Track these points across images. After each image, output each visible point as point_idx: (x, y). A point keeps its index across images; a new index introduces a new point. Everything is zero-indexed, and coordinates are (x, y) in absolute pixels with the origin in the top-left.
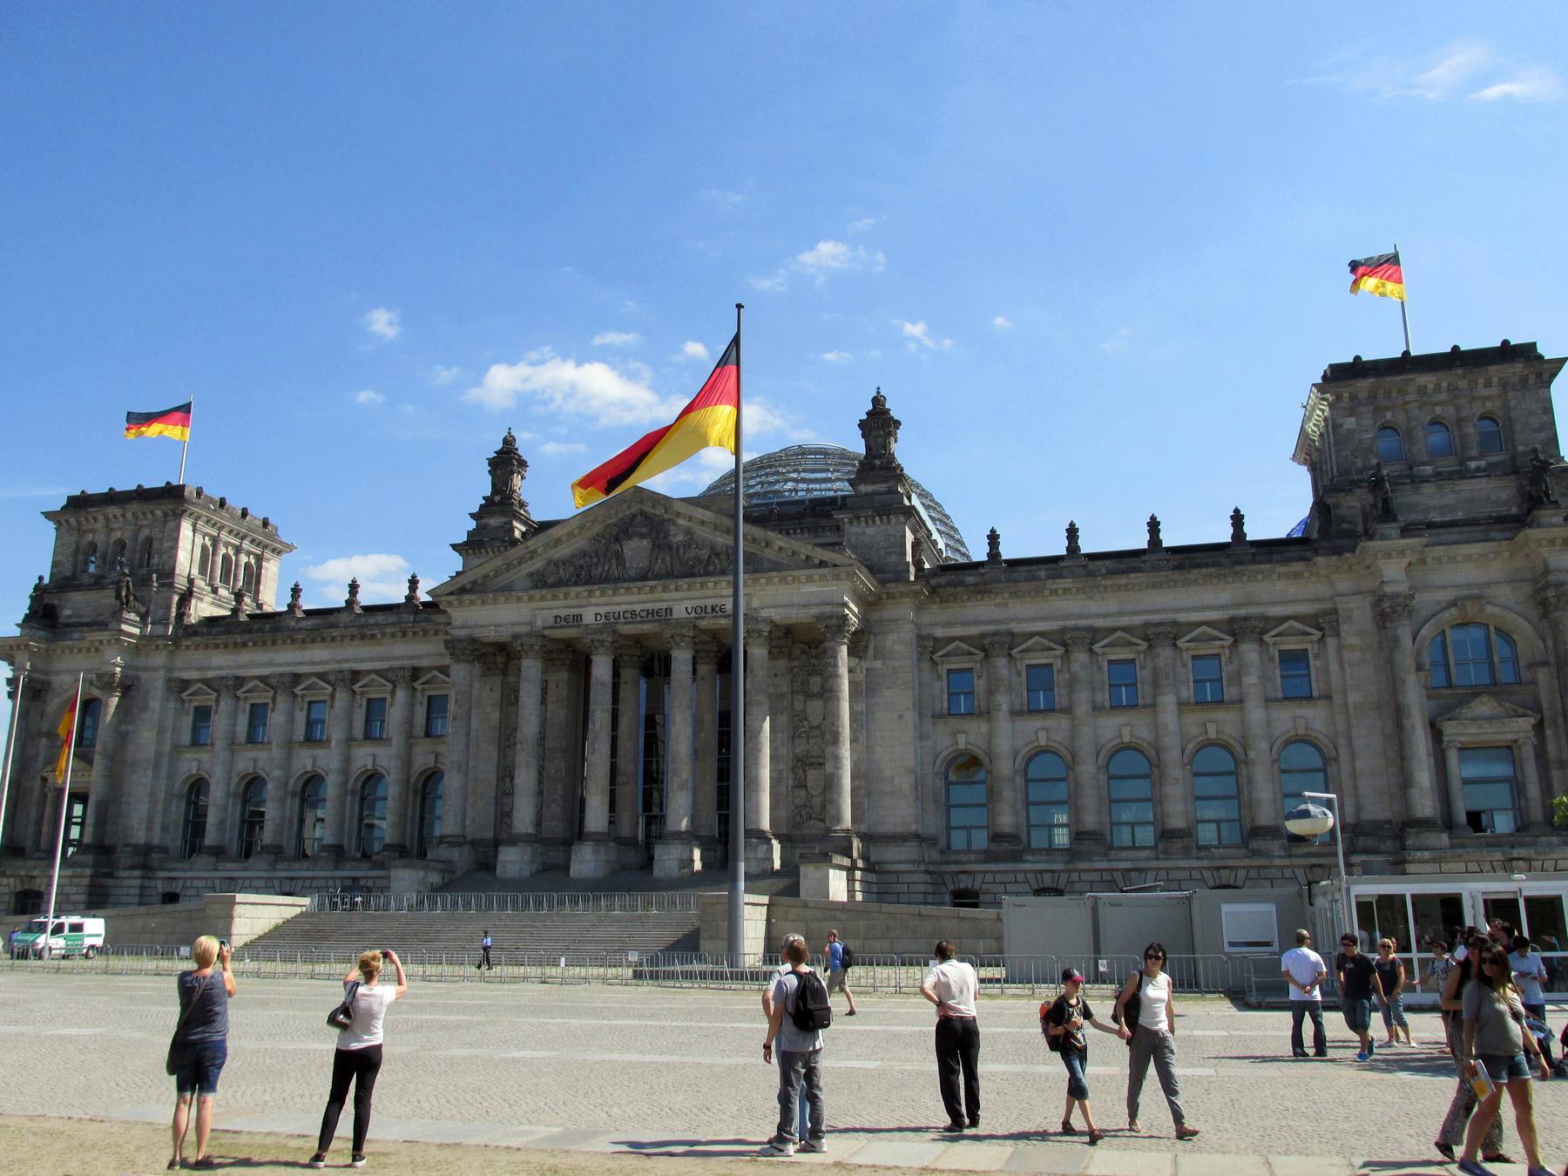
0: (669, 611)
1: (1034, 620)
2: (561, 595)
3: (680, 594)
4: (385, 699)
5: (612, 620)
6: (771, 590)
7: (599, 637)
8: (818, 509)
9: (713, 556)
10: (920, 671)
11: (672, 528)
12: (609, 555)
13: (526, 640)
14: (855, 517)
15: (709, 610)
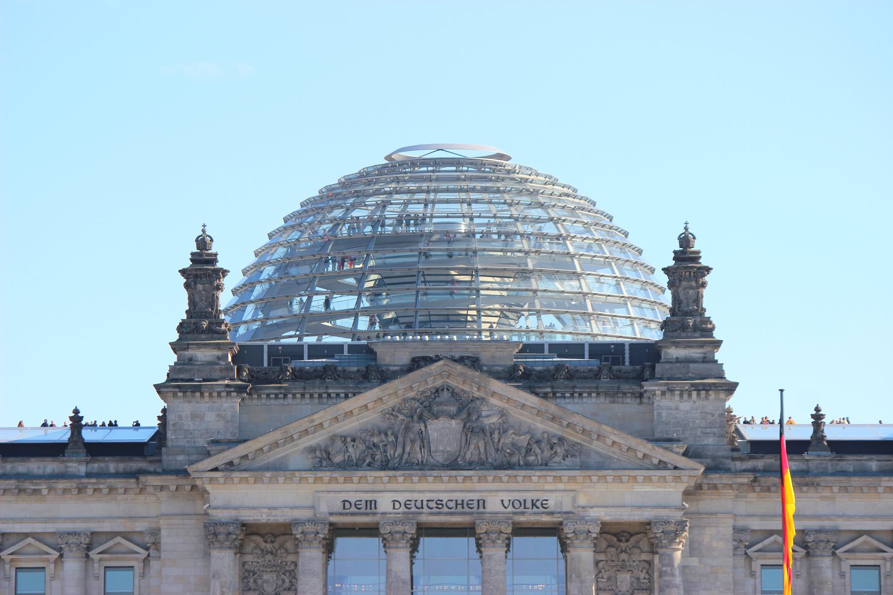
0: (482, 503)
1: (863, 517)
2: (356, 480)
3: (496, 486)
4: (44, 568)
5: (414, 509)
6: (601, 488)
7: (400, 528)
8: (615, 368)
9: (535, 446)
10: (735, 567)
11: (485, 408)
12: (412, 436)
13: (310, 528)
14: (668, 389)
15: (529, 504)
